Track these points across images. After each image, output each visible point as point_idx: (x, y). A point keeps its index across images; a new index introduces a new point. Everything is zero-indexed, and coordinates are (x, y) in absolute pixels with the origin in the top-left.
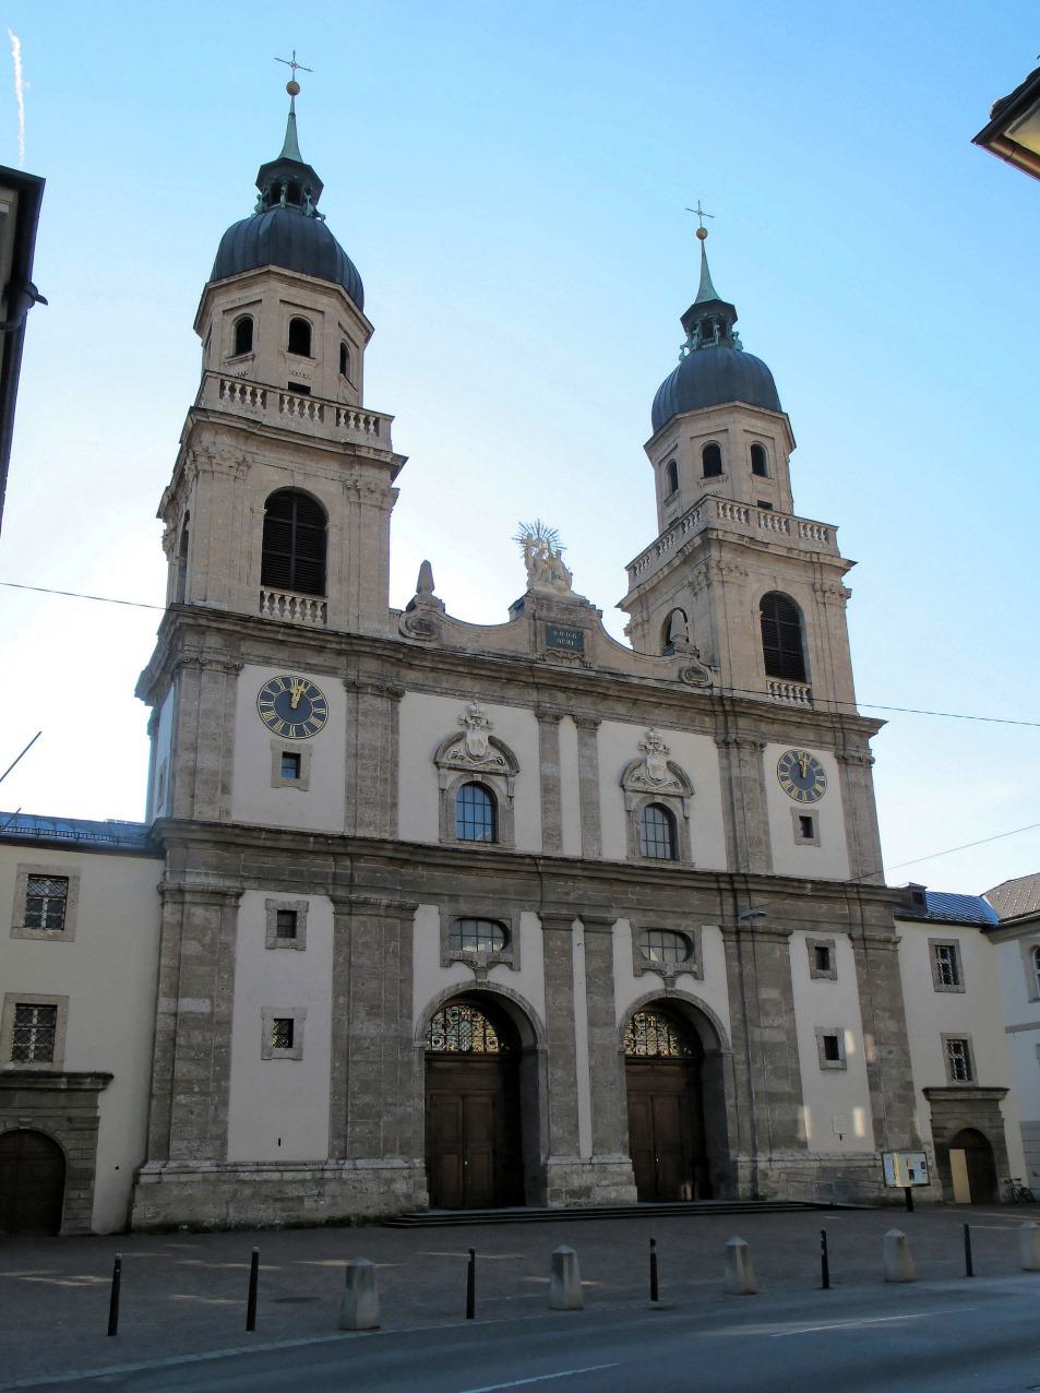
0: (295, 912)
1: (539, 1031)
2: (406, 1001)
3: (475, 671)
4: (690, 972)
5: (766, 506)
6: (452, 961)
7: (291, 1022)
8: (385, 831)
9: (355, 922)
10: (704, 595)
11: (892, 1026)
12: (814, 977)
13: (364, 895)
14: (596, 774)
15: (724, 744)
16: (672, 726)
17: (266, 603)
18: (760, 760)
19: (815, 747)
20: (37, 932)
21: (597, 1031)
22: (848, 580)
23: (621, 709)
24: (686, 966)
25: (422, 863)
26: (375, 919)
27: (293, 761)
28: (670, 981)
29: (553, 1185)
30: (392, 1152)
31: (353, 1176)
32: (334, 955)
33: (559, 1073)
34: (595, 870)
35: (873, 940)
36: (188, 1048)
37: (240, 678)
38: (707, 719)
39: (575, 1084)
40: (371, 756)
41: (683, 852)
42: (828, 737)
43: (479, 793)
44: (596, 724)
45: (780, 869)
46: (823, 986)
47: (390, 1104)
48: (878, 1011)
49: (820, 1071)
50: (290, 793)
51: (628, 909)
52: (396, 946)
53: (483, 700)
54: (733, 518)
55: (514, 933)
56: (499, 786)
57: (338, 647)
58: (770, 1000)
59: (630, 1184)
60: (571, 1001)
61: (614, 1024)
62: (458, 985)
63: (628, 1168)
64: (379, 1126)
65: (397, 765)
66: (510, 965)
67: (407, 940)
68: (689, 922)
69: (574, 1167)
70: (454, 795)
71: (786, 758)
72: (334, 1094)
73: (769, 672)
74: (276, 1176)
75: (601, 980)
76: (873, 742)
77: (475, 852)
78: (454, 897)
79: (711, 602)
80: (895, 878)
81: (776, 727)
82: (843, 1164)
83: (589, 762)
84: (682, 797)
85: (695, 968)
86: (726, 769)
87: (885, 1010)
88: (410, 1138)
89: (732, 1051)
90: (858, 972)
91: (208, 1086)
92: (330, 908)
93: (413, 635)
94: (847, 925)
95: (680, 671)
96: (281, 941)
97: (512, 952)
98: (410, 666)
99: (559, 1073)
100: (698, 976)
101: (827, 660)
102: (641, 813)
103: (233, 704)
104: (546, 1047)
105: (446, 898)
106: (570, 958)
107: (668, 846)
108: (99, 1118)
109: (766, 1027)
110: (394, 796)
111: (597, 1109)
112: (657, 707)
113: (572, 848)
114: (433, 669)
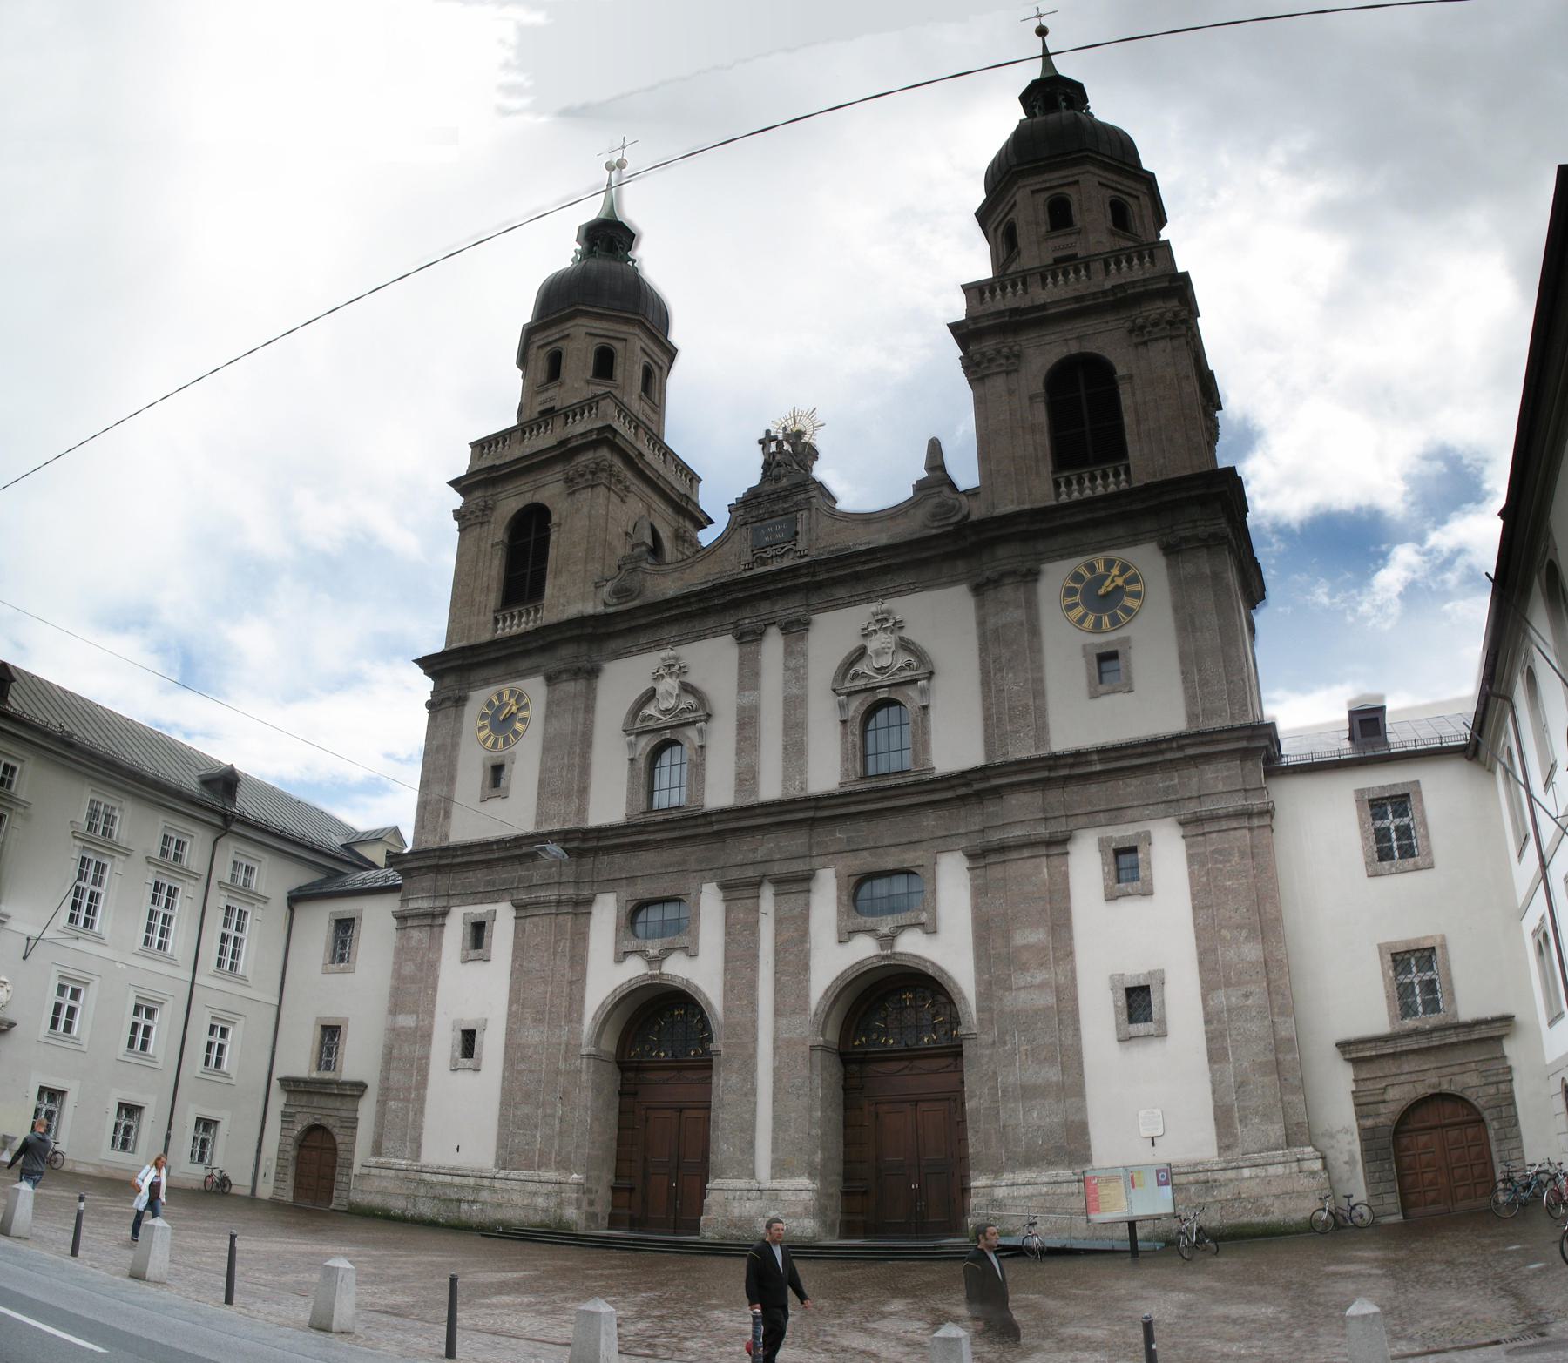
1: (714, 1028)
4: (920, 925)
6: (626, 954)
11: (1252, 952)
12: (1111, 897)
21: (784, 1021)
23: (841, 593)
27: (497, 772)
32: (513, 961)
33: (734, 1078)
34: (780, 813)
35: (1214, 818)
39: (753, 1091)
44: (808, 624)
58: (1027, 947)
61: (805, 1009)
62: (631, 980)
66: (684, 949)
68: (920, 853)
71: (1077, 577)
78: (631, 879)
83: (796, 673)
84: (915, 681)
85: (924, 917)
87: (1239, 927)
99: (734, 1078)
100: (930, 928)
104: (721, 1048)
105: (624, 881)
111: (778, 1123)
113: (770, 789)
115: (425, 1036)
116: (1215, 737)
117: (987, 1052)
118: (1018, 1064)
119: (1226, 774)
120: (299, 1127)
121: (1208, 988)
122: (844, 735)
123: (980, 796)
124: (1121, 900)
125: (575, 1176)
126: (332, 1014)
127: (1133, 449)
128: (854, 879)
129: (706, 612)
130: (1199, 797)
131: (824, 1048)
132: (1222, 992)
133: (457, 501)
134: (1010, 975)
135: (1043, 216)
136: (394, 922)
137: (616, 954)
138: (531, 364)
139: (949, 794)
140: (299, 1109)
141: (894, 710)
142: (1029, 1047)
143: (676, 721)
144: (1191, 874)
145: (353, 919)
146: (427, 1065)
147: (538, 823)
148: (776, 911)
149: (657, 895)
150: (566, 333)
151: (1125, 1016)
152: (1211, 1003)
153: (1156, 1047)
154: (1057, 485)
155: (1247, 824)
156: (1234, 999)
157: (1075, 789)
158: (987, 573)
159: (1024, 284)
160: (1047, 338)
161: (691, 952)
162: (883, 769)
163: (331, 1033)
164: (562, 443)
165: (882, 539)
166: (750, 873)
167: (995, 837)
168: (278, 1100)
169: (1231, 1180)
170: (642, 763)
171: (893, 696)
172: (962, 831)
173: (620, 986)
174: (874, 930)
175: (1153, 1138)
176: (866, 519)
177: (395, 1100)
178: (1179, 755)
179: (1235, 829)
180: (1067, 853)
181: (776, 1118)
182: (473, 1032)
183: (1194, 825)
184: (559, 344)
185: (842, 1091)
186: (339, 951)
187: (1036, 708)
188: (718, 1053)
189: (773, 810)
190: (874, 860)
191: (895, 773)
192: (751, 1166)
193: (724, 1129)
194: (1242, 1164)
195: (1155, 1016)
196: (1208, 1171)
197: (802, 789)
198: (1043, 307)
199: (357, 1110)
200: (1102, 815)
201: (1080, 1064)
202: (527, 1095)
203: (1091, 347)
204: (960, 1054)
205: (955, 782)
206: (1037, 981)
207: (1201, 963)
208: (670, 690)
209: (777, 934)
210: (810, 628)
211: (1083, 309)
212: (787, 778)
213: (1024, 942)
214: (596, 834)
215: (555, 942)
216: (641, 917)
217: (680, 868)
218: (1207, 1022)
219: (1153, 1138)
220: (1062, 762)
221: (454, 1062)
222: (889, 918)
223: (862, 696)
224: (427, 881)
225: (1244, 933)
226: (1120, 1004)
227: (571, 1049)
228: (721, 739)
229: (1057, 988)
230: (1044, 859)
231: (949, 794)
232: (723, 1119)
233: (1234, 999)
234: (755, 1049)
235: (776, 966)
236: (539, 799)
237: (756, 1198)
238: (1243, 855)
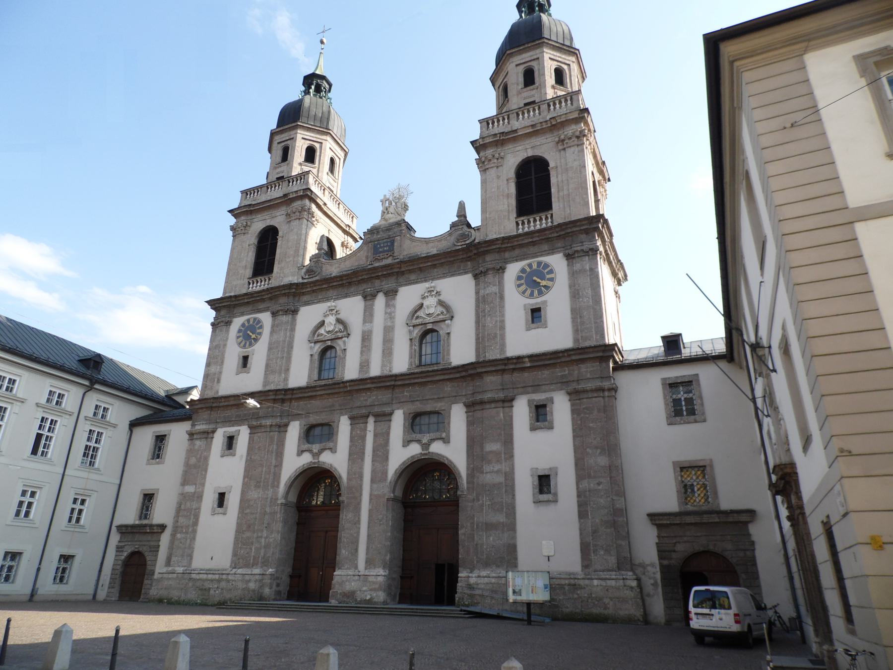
1: (342, 488)
2: (277, 477)
3: (331, 285)
6: (303, 451)
8: (279, 385)
9: (256, 437)
11: (603, 461)
12: (533, 429)
14: (393, 322)
15: (476, 276)
16: (444, 276)
21: (375, 486)
23: (413, 277)
24: (437, 435)
26: (264, 434)
27: (245, 359)
28: (426, 446)
35: (585, 391)
38: (469, 263)
39: (358, 522)
44: (397, 292)
47: (260, 537)
49: (533, 504)
50: (243, 376)
51: (401, 403)
52: (273, 448)
53: (335, 299)
55: (335, 430)
58: (491, 452)
59: (381, 590)
60: (361, 468)
64: (251, 549)
65: (292, 347)
66: (330, 449)
67: (281, 444)
68: (443, 404)
69: (349, 577)
71: (523, 270)
75: (382, 453)
83: (390, 315)
85: (444, 435)
87: (597, 448)
89: (465, 493)
92: (248, 431)
93: (307, 276)
94: (563, 384)
97: (333, 441)
98: (304, 294)
99: (350, 516)
100: (446, 440)
103: (227, 339)
112: (435, 268)
113: (375, 371)
114: (314, 291)
115: (199, 497)
116: (586, 350)
117: (470, 504)
118: (484, 511)
119: (591, 369)
120: (125, 554)
121: (579, 478)
122: (411, 346)
123: (473, 377)
124: (537, 431)
125: (270, 570)
126: (149, 487)
127: (555, 205)
128: (412, 415)
129: (350, 284)
130: (578, 380)
131: (394, 500)
132: (586, 481)
133: (232, 221)
134: (483, 466)
135: (521, 79)
136: (187, 436)
137: (298, 451)
138: (273, 152)
139: (458, 375)
140: (126, 543)
141: (435, 334)
142: (490, 503)
143: (333, 337)
144: (573, 419)
145: (165, 435)
146: (199, 512)
147: (264, 386)
148: (375, 430)
149: (319, 422)
150: (292, 137)
151: (537, 490)
152: (581, 486)
153: (552, 507)
154: (517, 224)
155: (602, 395)
156: (592, 485)
157: (518, 375)
158: (481, 269)
159: (508, 118)
160: (517, 148)
161: (333, 450)
162: (428, 362)
163: (148, 498)
164: (285, 195)
165: (434, 251)
166: (364, 411)
167: (478, 397)
168: (115, 538)
169: (587, 586)
170: (316, 357)
171: (435, 328)
172: (464, 394)
173: (299, 468)
174: (420, 440)
175: (549, 557)
176: (427, 241)
177: (180, 533)
178: (568, 359)
179: (596, 397)
180: (513, 406)
181: (369, 536)
182: (224, 493)
183: (575, 395)
184: (288, 142)
185: (403, 522)
186: (157, 453)
187: (500, 335)
188: (343, 502)
190: (421, 406)
191: (433, 364)
193: (344, 542)
194: (593, 577)
195: (552, 491)
196: (576, 579)
197: (390, 371)
198: (516, 131)
199: (159, 541)
201: (515, 513)
202: (249, 526)
203: (538, 152)
204: (457, 505)
205: (460, 370)
206: (496, 469)
207: (576, 465)
208: (332, 322)
209: (374, 442)
210: (398, 294)
211: (535, 132)
212: (383, 366)
213: (490, 449)
214: (291, 392)
215: (269, 445)
216: (312, 433)
218: (579, 496)
219: (549, 557)
220: (511, 361)
221: (213, 510)
222: (428, 435)
223: (421, 327)
224: (205, 415)
225: (599, 451)
226: (535, 484)
227: (274, 500)
228: (353, 346)
229: (505, 473)
230: (502, 409)
231: (458, 375)
232: (344, 536)
233: (592, 485)
234: (361, 500)
235: (373, 458)
236: (265, 374)
238: (599, 411)
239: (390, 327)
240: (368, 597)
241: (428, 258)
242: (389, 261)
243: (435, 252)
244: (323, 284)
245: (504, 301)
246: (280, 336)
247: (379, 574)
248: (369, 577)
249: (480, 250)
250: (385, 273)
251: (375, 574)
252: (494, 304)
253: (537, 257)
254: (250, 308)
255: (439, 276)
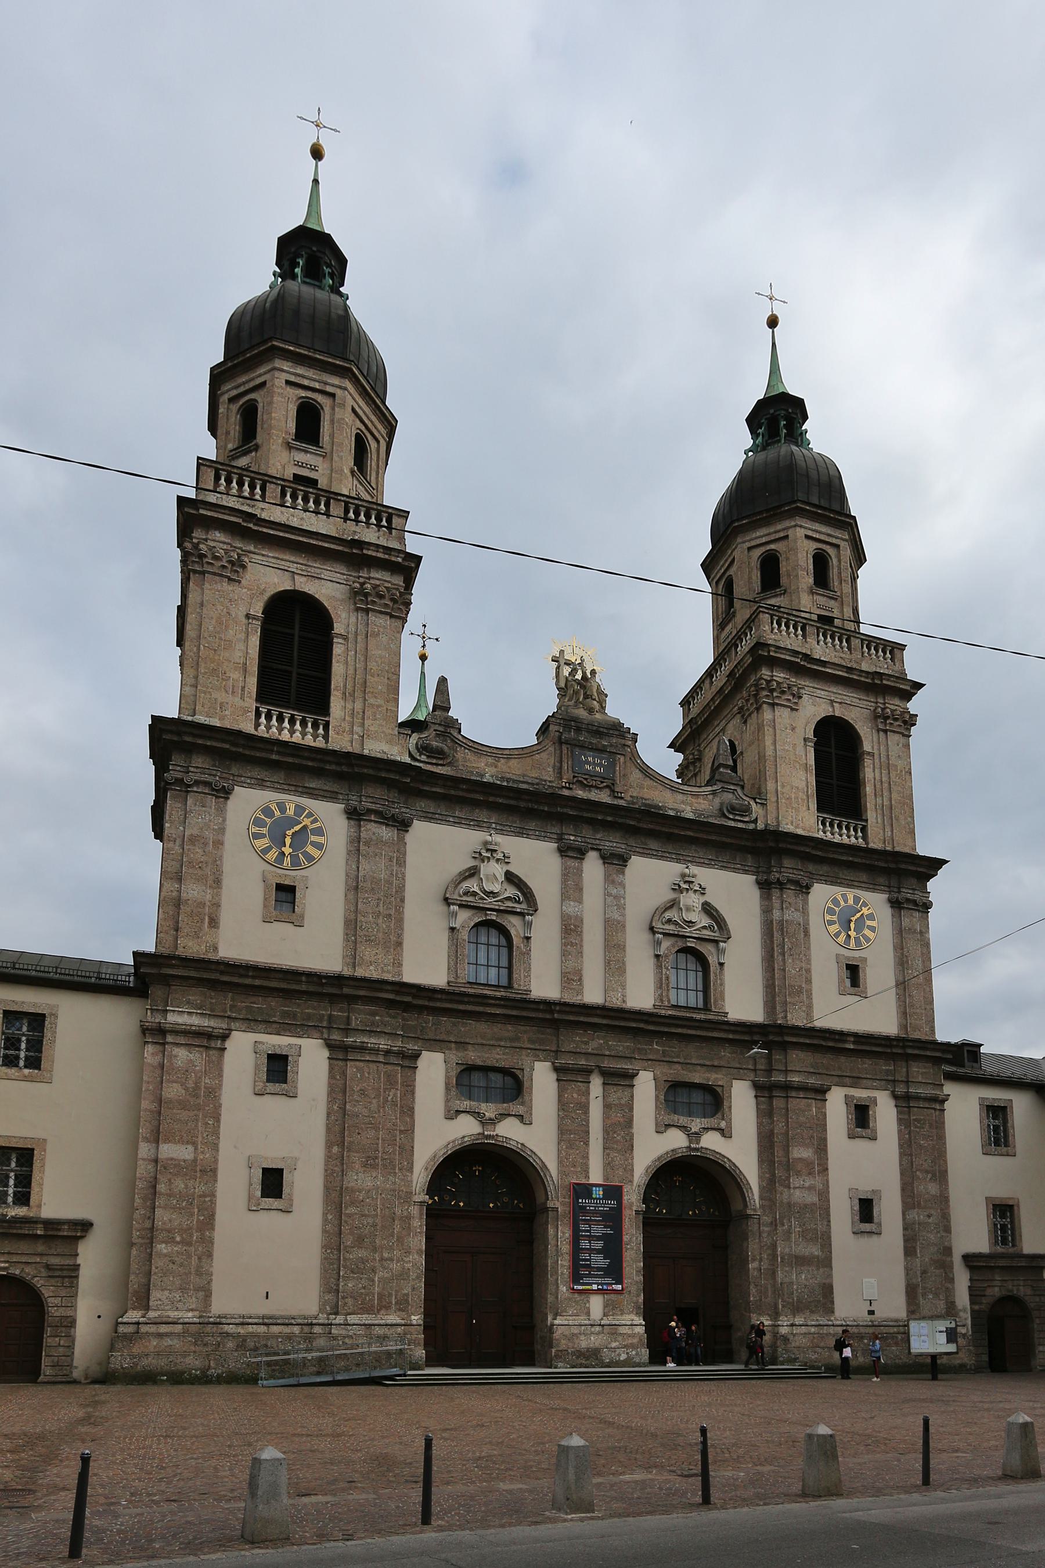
0: (287, 1056)
1: (551, 1188)
2: (408, 1151)
3: (491, 799)
5: (826, 620)
6: (458, 1112)
7: (280, 1171)
8: (388, 972)
10: (753, 720)
13: (360, 1039)
14: (624, 915)
15: (765, 886)
17: (263, 720)
18: (806, 902)
19: (867, 889)
20: (13, 1072)
22: (913, 706)
23: (653, 845)
25: (427, 1008)
29: (558, 1345)
30: (387, 1307)
31: (344, 1332)
36: (170, 1196)
37: (229, 802)
40: (373, 889)
41: (716, 1001)
42: (881, 880)
43: (494, 932)
44: (627, 861)
45: (821, 1022)
46: (861, 1145)
48: (918, 1173)
53: (501, 832)
54: (789, 634)
55: (526, 1085)
56: (514, 925)
57: (338, 769)
62: (464, 1137)
63: (641, 1330)
65: (403, 900)
66: (521, 1118)
67: (409, 1089)
69: (583, 1328)
70: (464, 935)
72: (325, 1247)
73: (820, 809)
74: (262, 1329)
76: (931, 885)
77: (485, 997)
78: (461, 1045)
79: (760, 728)
80: (946, 1033)
81: (825, 869)
82: (871, 1330)
83: (615, 899)
84: (716, 942)
86: (767, 911)
88: (407, 1295)
90: (900, 1131)
91: (191, 1236)
95: (722, 804)
96: (271, 1087)
97: (523, 1104)
101: (886, 794)
102: (672, 957)
104: (558, 1205)
105: (453, 1045)
106: (586, 1112)
107: (700, 994)
108: (79, 1265)
109: (795, 1188)
110: (400, 936)
113: (593, 994)
149: (489, 1063)
173: (454, 1141)
189: (612, 1014)
192: (587, 1305)
193: (562, 1273)
200: (847, 1079)
217: (514, 1045)
223: (672, 940)
237: (598, 1333)
239: (619, 922)
240: (623, 1357)
241: (679, 821)
242: (604, 797)
243: (690, 816)
244: (476, 792)
245: (809, 938)
246: (374, 867)
247: (635, 1323)
248: (620, 1328)
249: (780, 845)
250: (609, 819)
251: (629, 1323)
252: (797, 939)
253: (858, 887)
254: (279, 777)
255: (702, 861)
